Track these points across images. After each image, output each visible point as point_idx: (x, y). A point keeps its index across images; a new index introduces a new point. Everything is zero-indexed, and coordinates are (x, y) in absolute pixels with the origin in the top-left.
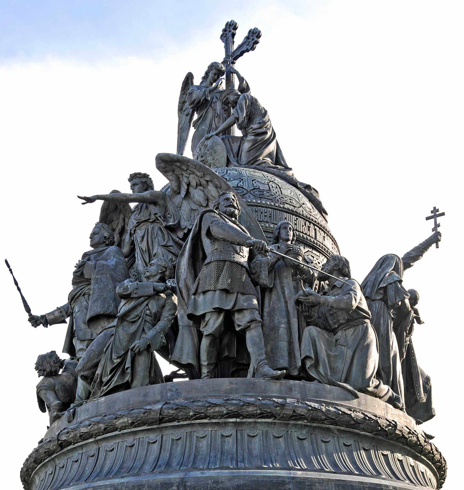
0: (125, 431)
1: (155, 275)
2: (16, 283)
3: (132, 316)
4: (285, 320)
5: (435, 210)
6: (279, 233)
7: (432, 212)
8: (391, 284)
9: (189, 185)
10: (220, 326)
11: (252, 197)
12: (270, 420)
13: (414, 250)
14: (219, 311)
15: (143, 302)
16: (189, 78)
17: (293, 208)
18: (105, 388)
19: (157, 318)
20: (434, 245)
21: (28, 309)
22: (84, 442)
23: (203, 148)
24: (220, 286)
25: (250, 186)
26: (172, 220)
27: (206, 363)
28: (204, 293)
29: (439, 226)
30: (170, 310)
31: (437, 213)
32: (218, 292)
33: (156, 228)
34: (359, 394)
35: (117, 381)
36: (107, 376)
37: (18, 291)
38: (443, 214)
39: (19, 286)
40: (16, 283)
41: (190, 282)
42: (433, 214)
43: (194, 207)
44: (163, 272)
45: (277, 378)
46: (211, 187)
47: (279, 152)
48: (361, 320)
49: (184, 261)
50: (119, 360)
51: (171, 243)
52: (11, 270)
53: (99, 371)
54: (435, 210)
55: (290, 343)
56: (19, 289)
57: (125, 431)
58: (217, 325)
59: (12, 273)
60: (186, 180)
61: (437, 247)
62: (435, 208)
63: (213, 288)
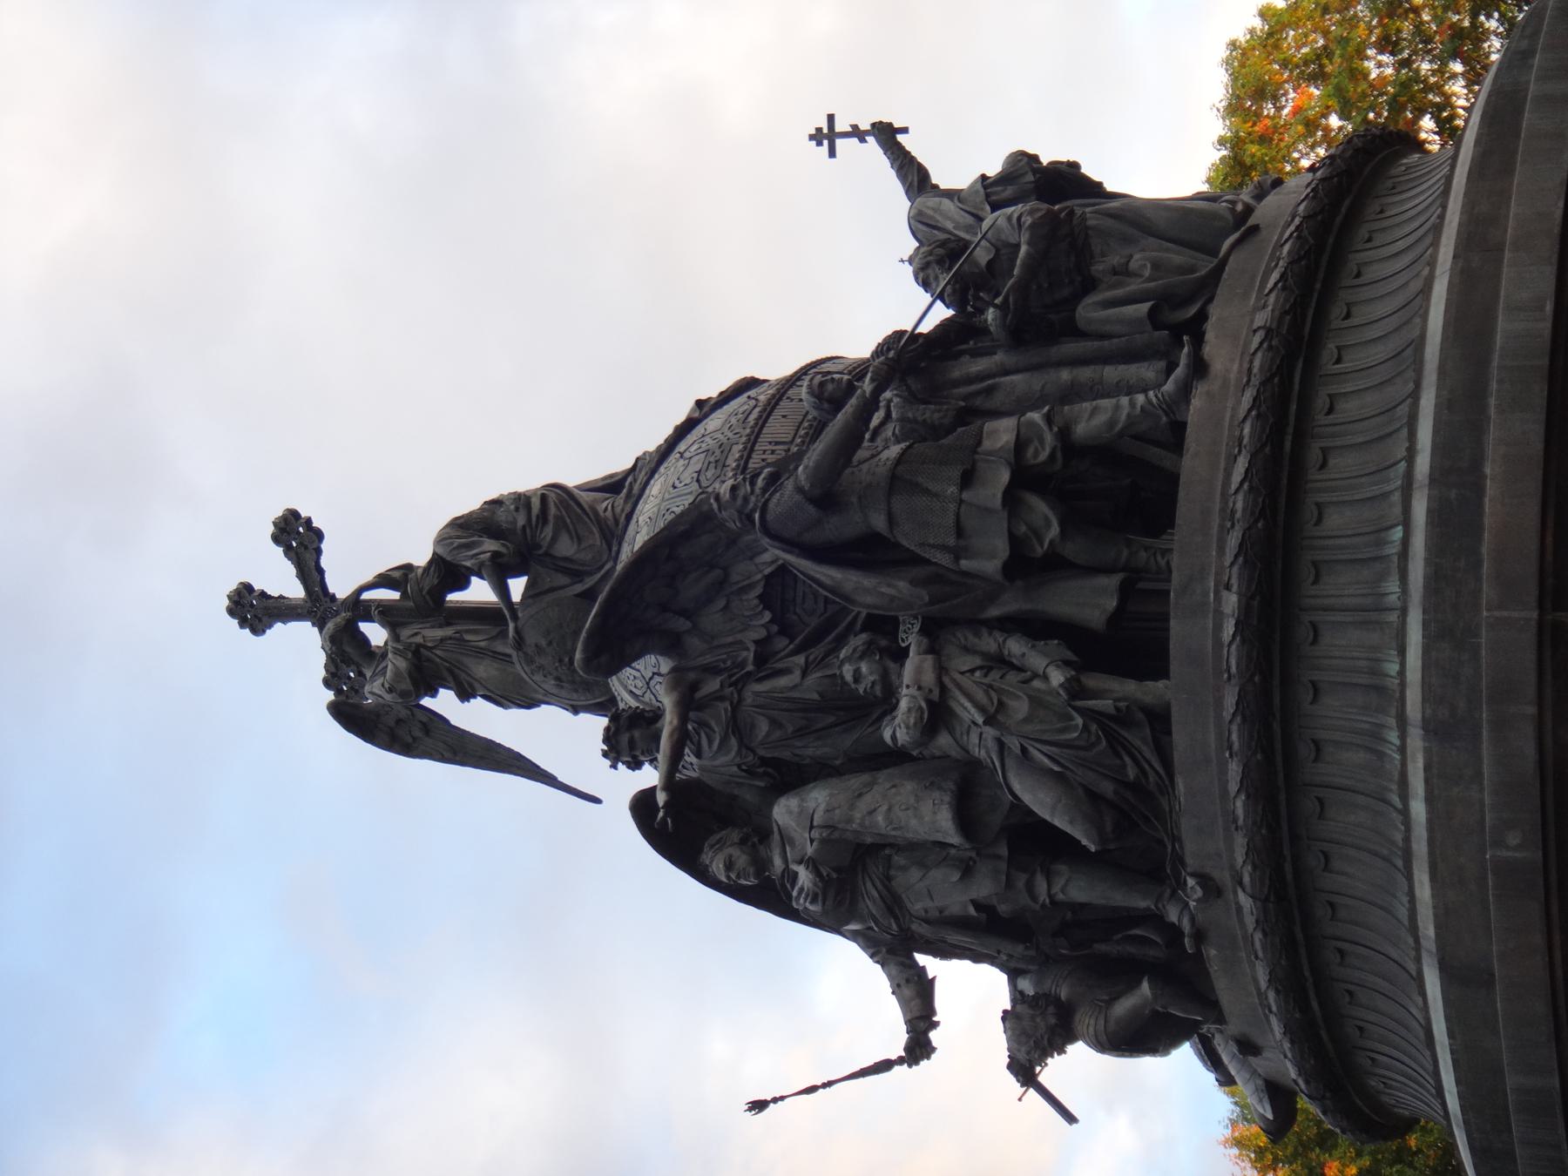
2: (812, 1090)
5: (817, 137)
7: (820, 144)
8: (987, 196)
17: (757, 410)
18: (1152, 778)
20: (900, 138)
21: (884, 1066)
22: (1285, 827)
23: (540, 661)
24: (952, 490)
25: (689, 490)
29: (855, 127)
31: (825, 131)
34: (1251, 222)
36: (1124, 766)
37: (834, 1087)
38: (831, 118)
39: (819, 1084)
40: (812, 1090)
42: (826, 142)
43: (722, 603)
44: (882, 651)
47: (588, 487)
48: (1075, 222)
51: (800, 659)
52: (775, 1100)
53: (1107, 788)
54: (817, 137)
59: (782, 1098)
61: (905, 130)
62: (812, 137)
63: (952, 507)
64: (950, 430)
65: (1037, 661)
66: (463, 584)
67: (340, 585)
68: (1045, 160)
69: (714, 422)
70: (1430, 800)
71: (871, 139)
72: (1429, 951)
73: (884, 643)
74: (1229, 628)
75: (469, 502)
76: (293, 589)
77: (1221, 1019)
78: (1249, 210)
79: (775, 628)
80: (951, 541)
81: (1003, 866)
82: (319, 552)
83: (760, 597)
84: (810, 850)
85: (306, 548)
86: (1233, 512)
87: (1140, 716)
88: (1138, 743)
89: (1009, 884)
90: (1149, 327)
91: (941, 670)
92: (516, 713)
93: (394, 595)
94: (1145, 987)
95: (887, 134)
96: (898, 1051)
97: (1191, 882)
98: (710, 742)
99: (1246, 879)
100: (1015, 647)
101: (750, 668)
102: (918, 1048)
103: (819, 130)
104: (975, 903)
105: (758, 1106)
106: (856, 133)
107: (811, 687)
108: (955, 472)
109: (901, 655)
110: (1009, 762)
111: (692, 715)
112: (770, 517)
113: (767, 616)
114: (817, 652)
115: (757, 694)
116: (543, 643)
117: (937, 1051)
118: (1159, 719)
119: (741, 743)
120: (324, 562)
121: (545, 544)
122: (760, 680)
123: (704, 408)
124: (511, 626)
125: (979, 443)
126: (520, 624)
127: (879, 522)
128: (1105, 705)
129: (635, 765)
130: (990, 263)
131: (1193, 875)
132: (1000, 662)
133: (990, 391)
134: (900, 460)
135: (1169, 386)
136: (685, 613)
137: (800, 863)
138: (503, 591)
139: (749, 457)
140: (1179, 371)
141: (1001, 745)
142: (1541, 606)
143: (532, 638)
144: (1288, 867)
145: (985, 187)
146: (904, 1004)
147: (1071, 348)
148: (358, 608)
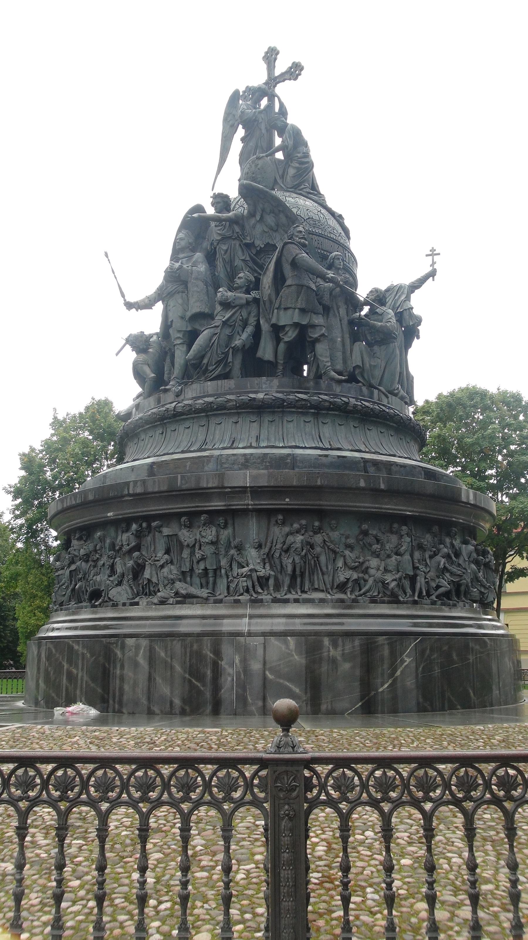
0: (232, 411)
1: (243, 287)
3: (231, 321)
4: (340, 335)
5: (433, 250)
6: (333, 262)
8: (406, 310)
9: (263, 210)
10: (297, 336)
11: (308, 225)
12: (337, 413)
13: (417, 281)
14: (296, 325)
15: (238, 310)
20: (431, 278)
21: (123, 295)
22: (196, 415)
23: (253, 166)
24: (299, 305)
26: (248, 238)
27: (282, 362)
28: (286, 309)
29: (435, 263)
30: (254, 316)
32: (297, 310)
33: (237, 245)
35: (220, 371)
38: (439, 254)
41: (273, 297)
43: (266, 230)
44: (248, 286)
45: (339, 382)
46: (282, 215)
49: (267, 280)
50: (223, 356)
51: (248, 259)
53: (205, 361)
54: (433, 250)
55: (344, 353)
56: (116, 278)
57: (232, 411)
58: (294, 335)
60: (261, 206)
61: (433, 280)
63: (293, 306)
64: (320, 304)
65: (244, 336)
66: (280, 136)
67: (281, 89)
68: (419, 328)
69: (332, 222)
71: (431, 268)
73: (251, 286)
74: (253, 396)
75: (306, 135)
76: (277, 73)
77: (144, 399)
78: (396, 395)
79: (258, 249)
80: (282, 306)
81: (184, 329)
82: (290, 79)
83: (268, 243)
84: (185, 266)
85: (291, 75)
86: (289, 395)
87: (228, 370)
88: (220, 369)
89: (179, 331)
90: (354, 365)
91: (241, 306)
93: (277, 109)
94: (153, 375)
95: (432, 274)
96: (128, 299)
97: (180, 388)
98: (219, 230)
99: (180, 405)
100: (250, 329)
101: (244, 241)
102: (129, 306)
103: (435, 250)
104: (172, 321)
105: (106, 255)
106: (434, 263)
107: (238, 263)
108: (303, 306)
109: (248, 292)
110: (212, 330)
111: (228, 223)
112: (290, 245)
113: (263, 246)
114: (251, 264)
115: (235, 245)
116: (259, 167)
118: (226, 376)
119: (219, 241)
120: (287, 81)
121: (292, 164)
122: (240, 245)
123: (339, 219)
124: (264, 155)
125: (315, 313)
126: (266, 158)
127: (289, 282)
128: (230, 359)
129: (213, 204)
130: (377, 313)
132: (245, 324)
133: (335, 315)
134: (309, 288)
135: (333, 373)
136: (262, 217)
137: (182, 263)
138: (278, 150)
139: (317, 235)
140: (337, 376)
141: (218, 327)
142: (250, 487)
143: (260, 162)
144: (185, 417)
145: (409, 309)
146: (143, 300)
147: (348, 341)
148: (272, 97)
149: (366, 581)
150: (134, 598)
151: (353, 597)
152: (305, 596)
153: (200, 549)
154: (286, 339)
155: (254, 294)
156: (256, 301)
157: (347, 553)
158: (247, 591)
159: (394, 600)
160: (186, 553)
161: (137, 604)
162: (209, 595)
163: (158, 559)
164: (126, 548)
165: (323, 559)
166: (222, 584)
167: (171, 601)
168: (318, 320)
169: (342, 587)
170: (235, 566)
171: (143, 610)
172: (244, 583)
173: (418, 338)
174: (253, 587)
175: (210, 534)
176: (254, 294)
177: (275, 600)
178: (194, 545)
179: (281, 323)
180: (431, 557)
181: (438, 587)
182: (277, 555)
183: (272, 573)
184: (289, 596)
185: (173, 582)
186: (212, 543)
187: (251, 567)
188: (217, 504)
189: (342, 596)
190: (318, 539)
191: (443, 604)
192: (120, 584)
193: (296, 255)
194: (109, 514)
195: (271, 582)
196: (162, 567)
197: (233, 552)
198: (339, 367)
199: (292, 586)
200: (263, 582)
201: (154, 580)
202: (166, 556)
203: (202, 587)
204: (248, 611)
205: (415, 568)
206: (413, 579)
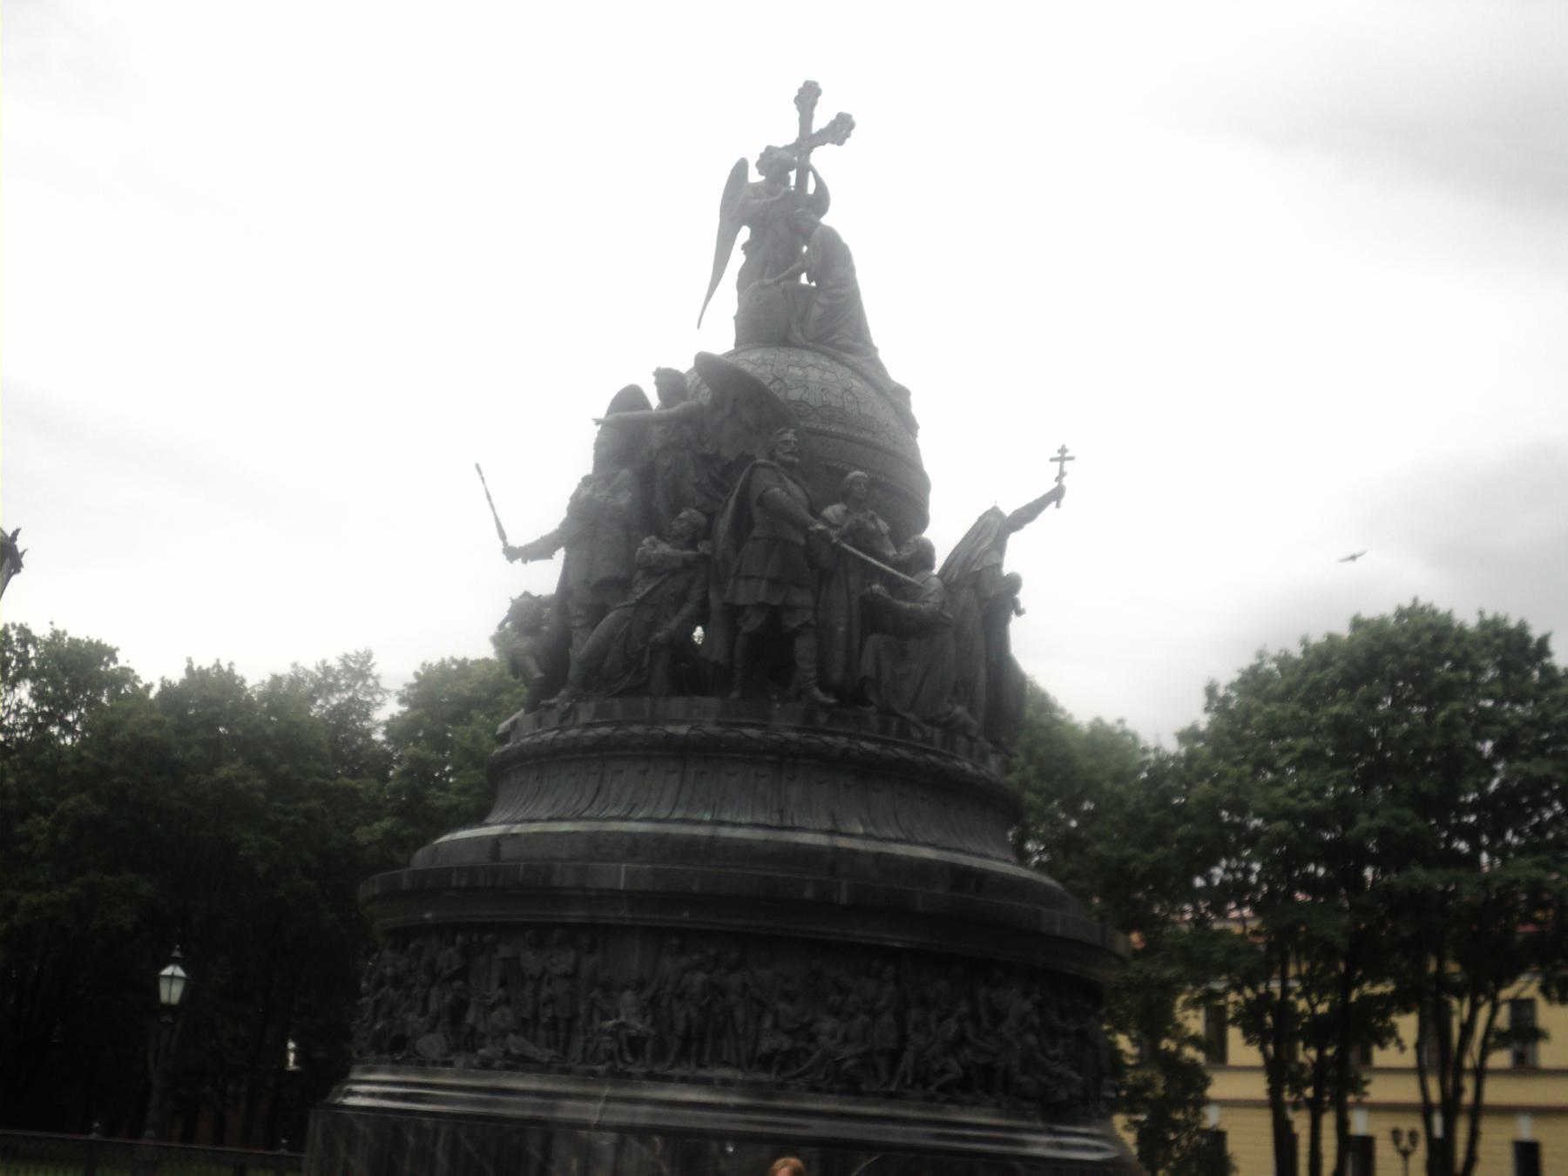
5: (1063, 450)
7: (1059, 451)
14: (762, 606)
16: (741, 168)
19: (682, 598)
20: (1054, 504)
28: (748, 578)
31: (1067, 455)
42: (1059, 455)
52: (482, 478)
54: (1063, 450)
58: (759, 623)
59: (483, 482)
61: (1058, 506)
62: (1063, 447)
70: (567, 833)
71: (1057, 484)
72: (510, 829)
74: (670, 729)
92: (736, 278)
95: (1056, 495)
97: (568, 704)
102: (512, 553)
106: (1062, 474)
109: (692, 544)
117: (508, 562)
118: (636, 691)
127: (756, 532)
131: (571, 707)
135: (817, 692)
148: (804, 170)
149: (809, 1054)
150: (447, 1055)
151: (780, 1079)
152: (702, 1073)
153: (549, 984)
154: (746, 628)
155: (703, 548)
156: (704, 558)
157: (782, 1006)
158: (611, 1057)
159: (852, 1089)
160: (528, 989)
161: (450, 1064)
162: (555, 1059)
163: (488, 994)
164: (446, 973)
165: (740, 1014)
166: (578, 1041)
167: (497, 1063)
168: (802, 598)
169: (765, 1062)
170: (596, 1018)
171: (457, 1076)
172: (607, 1043)
173: (1019, 613)
174: (621, 1051)
175: (563, 961)
176: (703, 548)
177: (651, 1076)
178: (541, 978)
179: (741, 601)
180: (940, 1020)
181: (943, 1071)
182: (665, 1003)
183: (652, 1032)
184: (677, 1072)
185: (504, 1033)
186: (566, 976)
187: (622, 1019)
188: (577, 915)
189: (763, 1077)
190: (735, 980)
191: (950, 1101)
192: (432, 1029)
193: (766, 490)
194: (428, 915)
195: (649, 1046)
196: (493, 1007)
197: (596, 993)
198: (837, 676)
199: (683, 1055)
200: (636, 1045)
201: (481, 1027)
202: (501, 992)
203: (549, 1045)
204: (607, 1091)
205: (903, 1038)
206: (895, 1057)
